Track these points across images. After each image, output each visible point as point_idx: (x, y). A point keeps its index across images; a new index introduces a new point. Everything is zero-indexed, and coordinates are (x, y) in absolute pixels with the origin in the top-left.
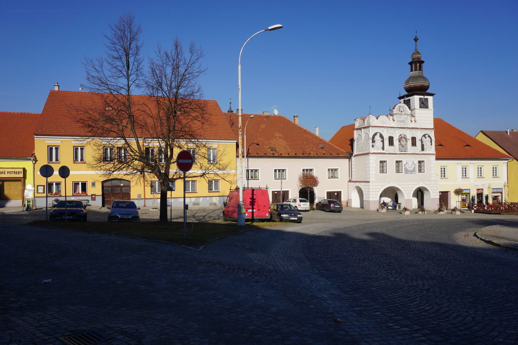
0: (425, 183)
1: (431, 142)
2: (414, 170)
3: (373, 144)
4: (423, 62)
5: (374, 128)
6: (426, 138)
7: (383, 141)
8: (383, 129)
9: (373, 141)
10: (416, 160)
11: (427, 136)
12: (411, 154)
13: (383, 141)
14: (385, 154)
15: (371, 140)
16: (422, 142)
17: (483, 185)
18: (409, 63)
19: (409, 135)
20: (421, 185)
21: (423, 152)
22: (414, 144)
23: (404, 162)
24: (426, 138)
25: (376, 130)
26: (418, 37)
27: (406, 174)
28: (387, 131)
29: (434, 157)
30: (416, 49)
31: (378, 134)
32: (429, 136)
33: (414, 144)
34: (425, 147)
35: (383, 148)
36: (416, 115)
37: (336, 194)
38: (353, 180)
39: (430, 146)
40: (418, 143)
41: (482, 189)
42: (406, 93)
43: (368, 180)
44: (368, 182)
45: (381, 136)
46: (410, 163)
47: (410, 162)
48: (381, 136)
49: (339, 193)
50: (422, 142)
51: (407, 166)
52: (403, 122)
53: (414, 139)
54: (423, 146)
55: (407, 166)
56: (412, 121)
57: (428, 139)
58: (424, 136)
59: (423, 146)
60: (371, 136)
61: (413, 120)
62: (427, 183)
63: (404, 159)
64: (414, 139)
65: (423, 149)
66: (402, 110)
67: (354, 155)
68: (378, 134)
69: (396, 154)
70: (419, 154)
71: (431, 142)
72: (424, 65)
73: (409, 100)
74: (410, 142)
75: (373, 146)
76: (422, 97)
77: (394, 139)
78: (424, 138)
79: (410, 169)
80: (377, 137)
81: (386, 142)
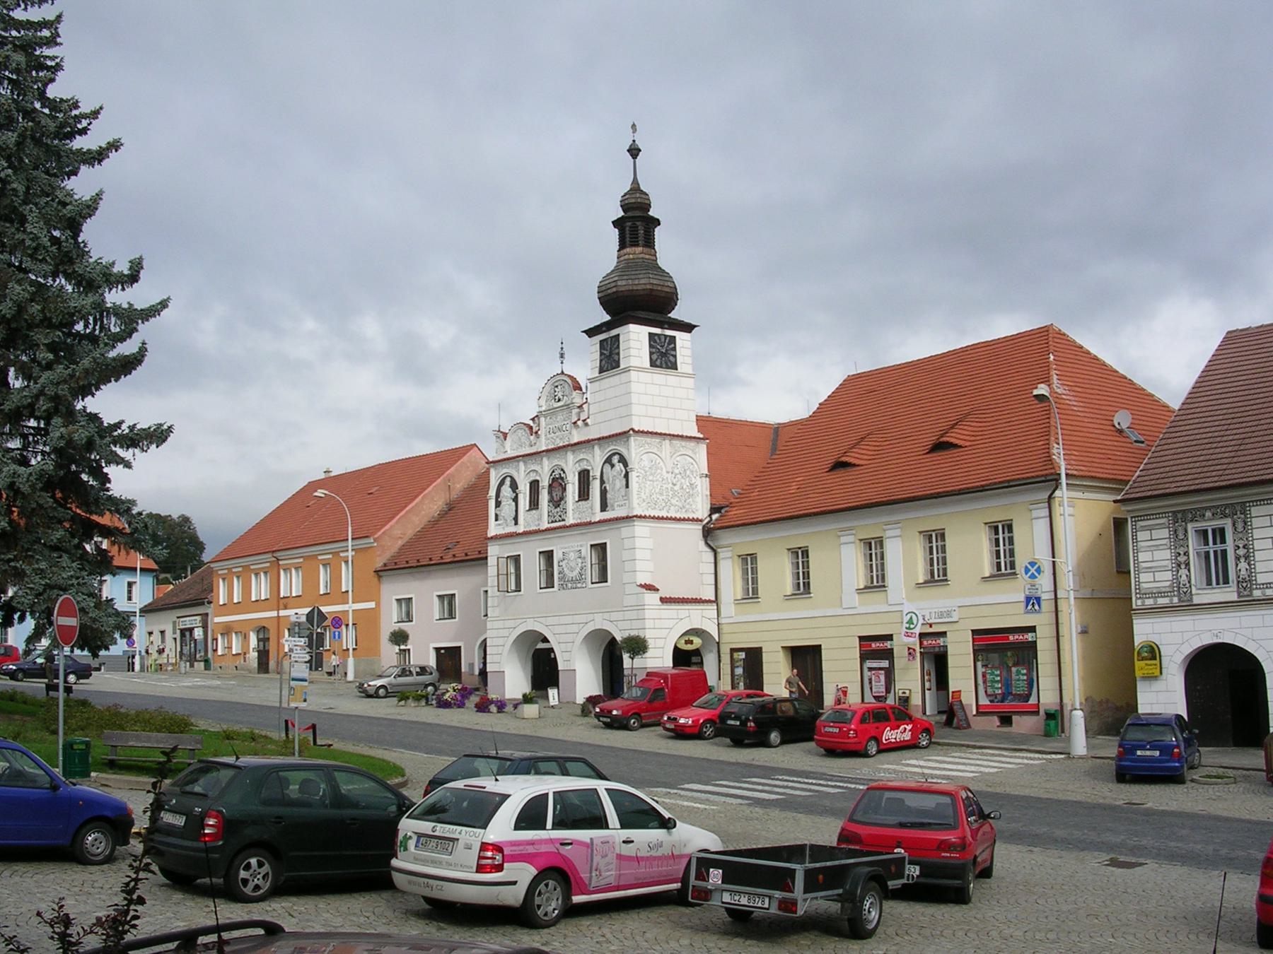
0: (606, 616)
2: (580, 578)
11: (615, 459)
12: (599, 522)
17: (941, 615)
21: (606, 515)
22: (584, 494)
24: (613, 466)
26: (640, 144)
30: (635, 181)
31: (508, 481)
34: (608, 496)
39: (623, 489)
41: (944, 634)
46: (572, 556)
51: (563, 564)
53: (584, 477)
54: (604, 493)
55: (563, 564)
57: (619, 467)
58: (608, 461)
62: (614, 616)
65: (604, 507)
66: (560, 395)
68: (508, 481)
78: (608, 466)
81: (524, 501)
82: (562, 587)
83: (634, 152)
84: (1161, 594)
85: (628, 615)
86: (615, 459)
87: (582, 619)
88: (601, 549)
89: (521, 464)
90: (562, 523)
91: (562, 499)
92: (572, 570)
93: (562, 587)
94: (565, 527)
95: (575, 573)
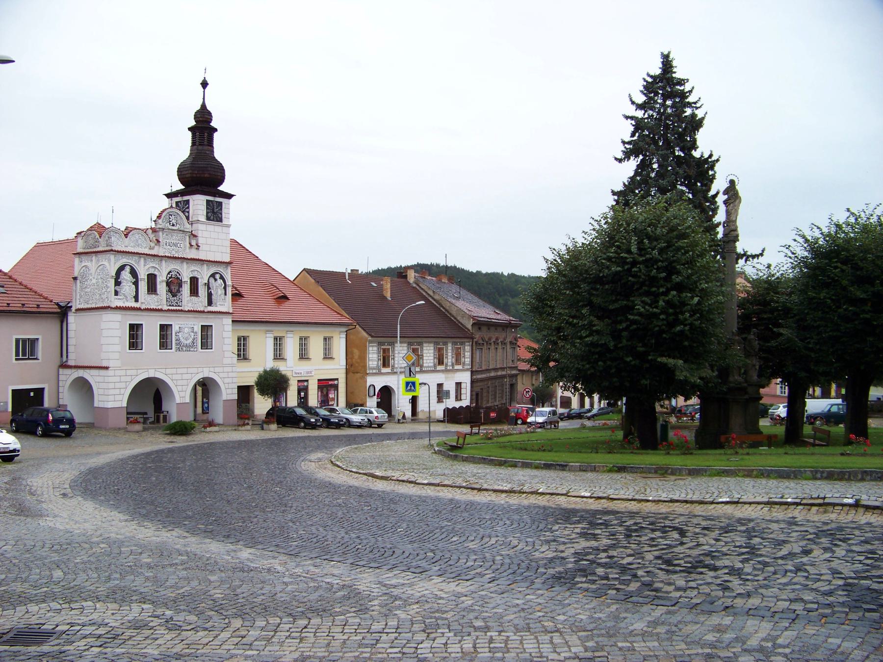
0: (212, 369)
1: (225, 288)
3: (117, 288)
4: (216, 130)
5: (119, 256)
6: (216, 280)
7: (136, 284)
8: (136, 258)
9: (118, 283)
10: (196, 324)
11: (218, 276)
12: (189, 311)
13: (136, 284)
14: (139, 309)
15: (112, 282)
16: (209, 288)
17: (308, 373)
18: (189, 129)
19: (186, 273)
20: (206, 373)
22: (194, 292)
23: (175, 328)
24: (216, 280)
25: (124, 260)
27: (178, 352)
28: (145, 262)
29: (228, 320)
31: (128, 269)
32: (222, 278)
33: (194, 292)
34: (213, 297)
35: (137, 300)
36: (200, 234)
37: (32, 394)
38: (71, 363)
39: (223, 296)
40: (202, 291)
41: (307, 381)
42: (181, 187)
43: (104, 364)
44: (107, 368)
45: (134, 273)
47: (186, 328)
48: (134, 273)
49: (40, 392)
50: (209, 288)
51: (180, 335)
52: (175, 245)
53: (194, 281)
54: (210, 295)
55: (180, 335)
56: (191, 245)
57: (220, 281)
58: (213, 275)
59: (210, 295)
60: (113, 273)
61: (194, 243)
62: (217, 370)
63: (177, 323)
64: (194, 281)
65: (210, 303)
66: (174, 221)
67: (73, 309)
68: (128, 269)
69: (161, 310)
70: (203, 312)
71: (225, 288)
72: (216, 135)
73: (188, 202)
74: (186, 289)
75: (116, 293)
76: (210, 198)
77: (159, 280)
78: (212, 280)
79: (186, 342)
80: (126, 275)
81: (143, 286)
82: (178, 349)
83: (204, 84)
84: (374, 369)
85: (226, 369)
86: (218, 276)
87: (195, 370)
88: (206, 330)
89: (142, 260)
90: (178, 308)
91: (179, 291)
92: (187, 339)
93: (178, 349)
94: (182, 311)
95: (189, 341)
